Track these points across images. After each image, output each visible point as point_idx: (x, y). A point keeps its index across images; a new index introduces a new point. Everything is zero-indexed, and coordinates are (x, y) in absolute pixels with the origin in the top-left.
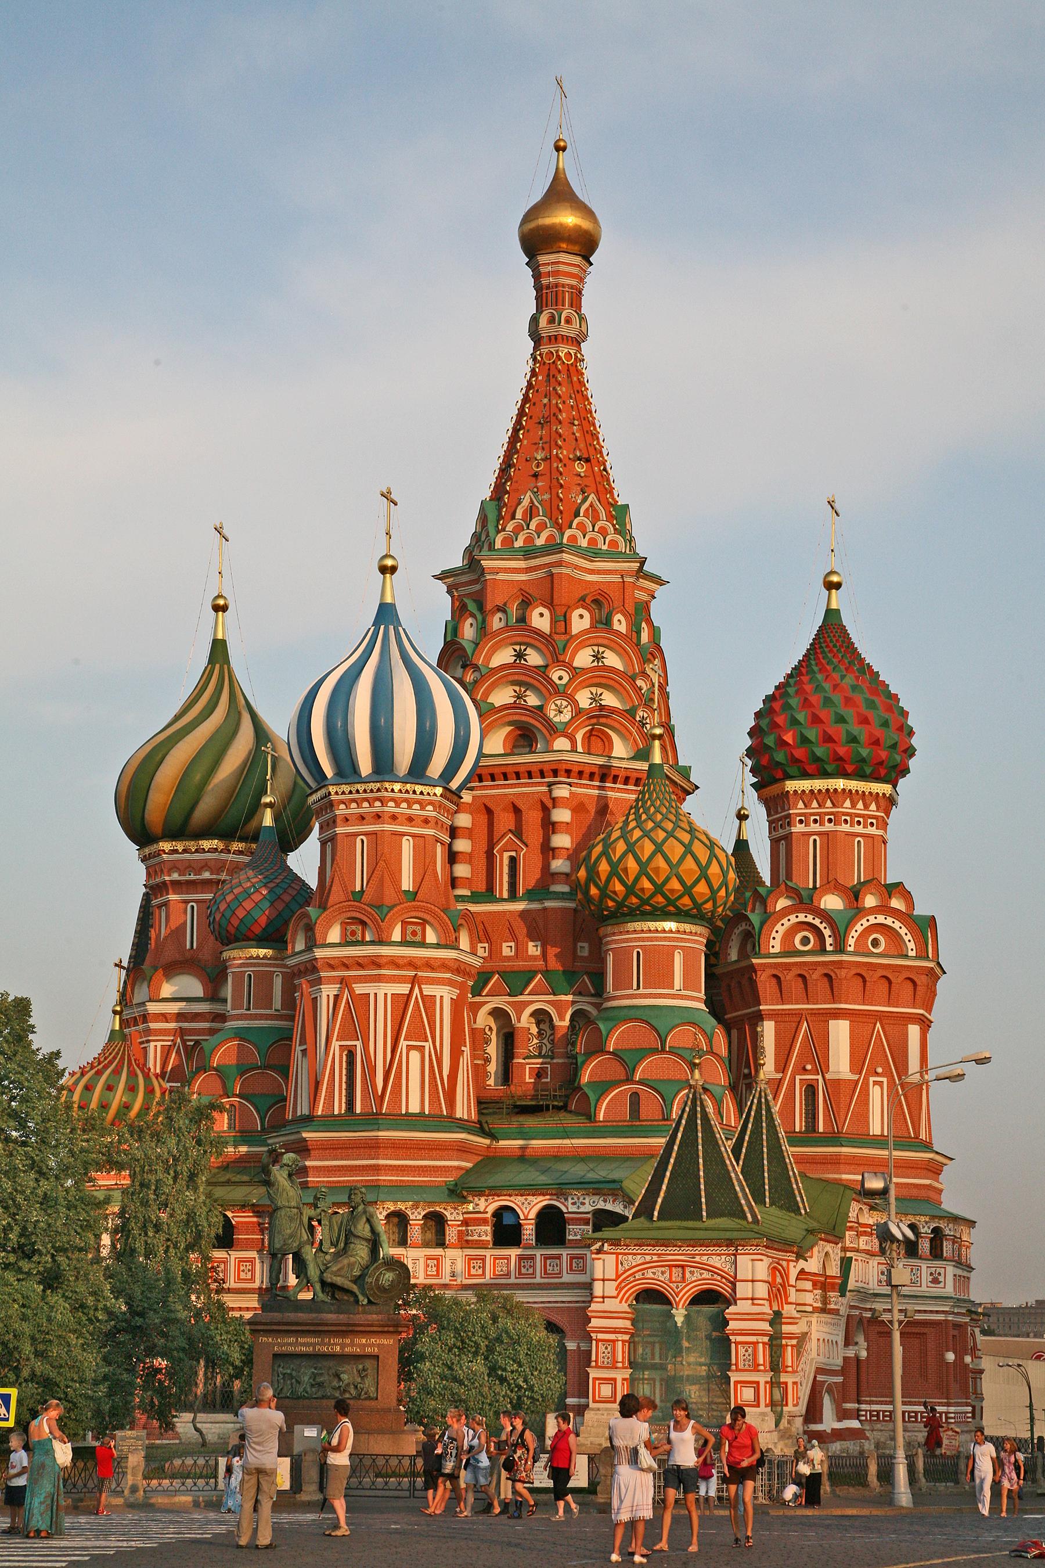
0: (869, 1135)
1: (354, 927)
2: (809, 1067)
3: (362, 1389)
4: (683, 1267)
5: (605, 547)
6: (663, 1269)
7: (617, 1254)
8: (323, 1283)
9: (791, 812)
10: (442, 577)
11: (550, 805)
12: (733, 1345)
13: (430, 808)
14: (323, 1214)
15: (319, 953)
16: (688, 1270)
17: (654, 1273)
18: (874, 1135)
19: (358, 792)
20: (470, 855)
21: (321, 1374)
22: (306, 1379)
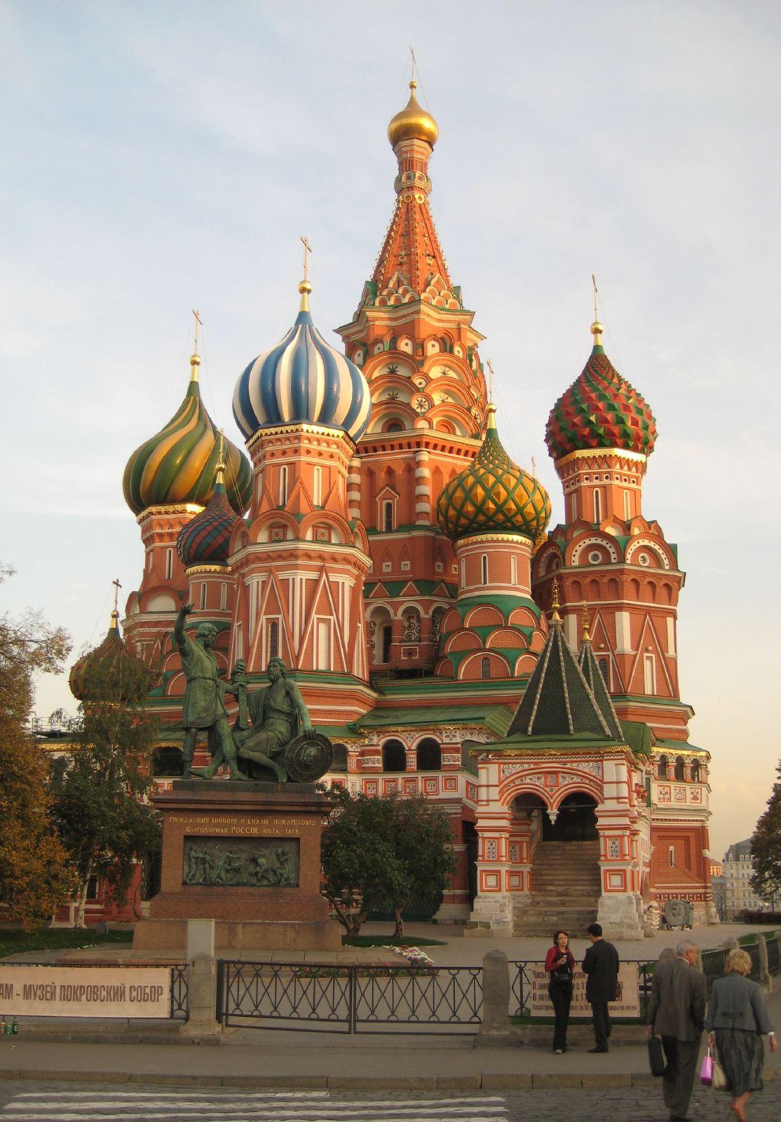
0: (644, 694)
1: (276, 530)
2: (602, 646)
3: (282, 875)
6: (539, 775)
9: (580, 472)
10: (338, 331)
11: (413, 465)
12: (602, 840)
13: (334, 446)
14: (240, 689)
15: (251, 549)
16: (560, 775)
19: (282, 432)
20: (359, 503)
21: (238, 858)
22: (221, 863)
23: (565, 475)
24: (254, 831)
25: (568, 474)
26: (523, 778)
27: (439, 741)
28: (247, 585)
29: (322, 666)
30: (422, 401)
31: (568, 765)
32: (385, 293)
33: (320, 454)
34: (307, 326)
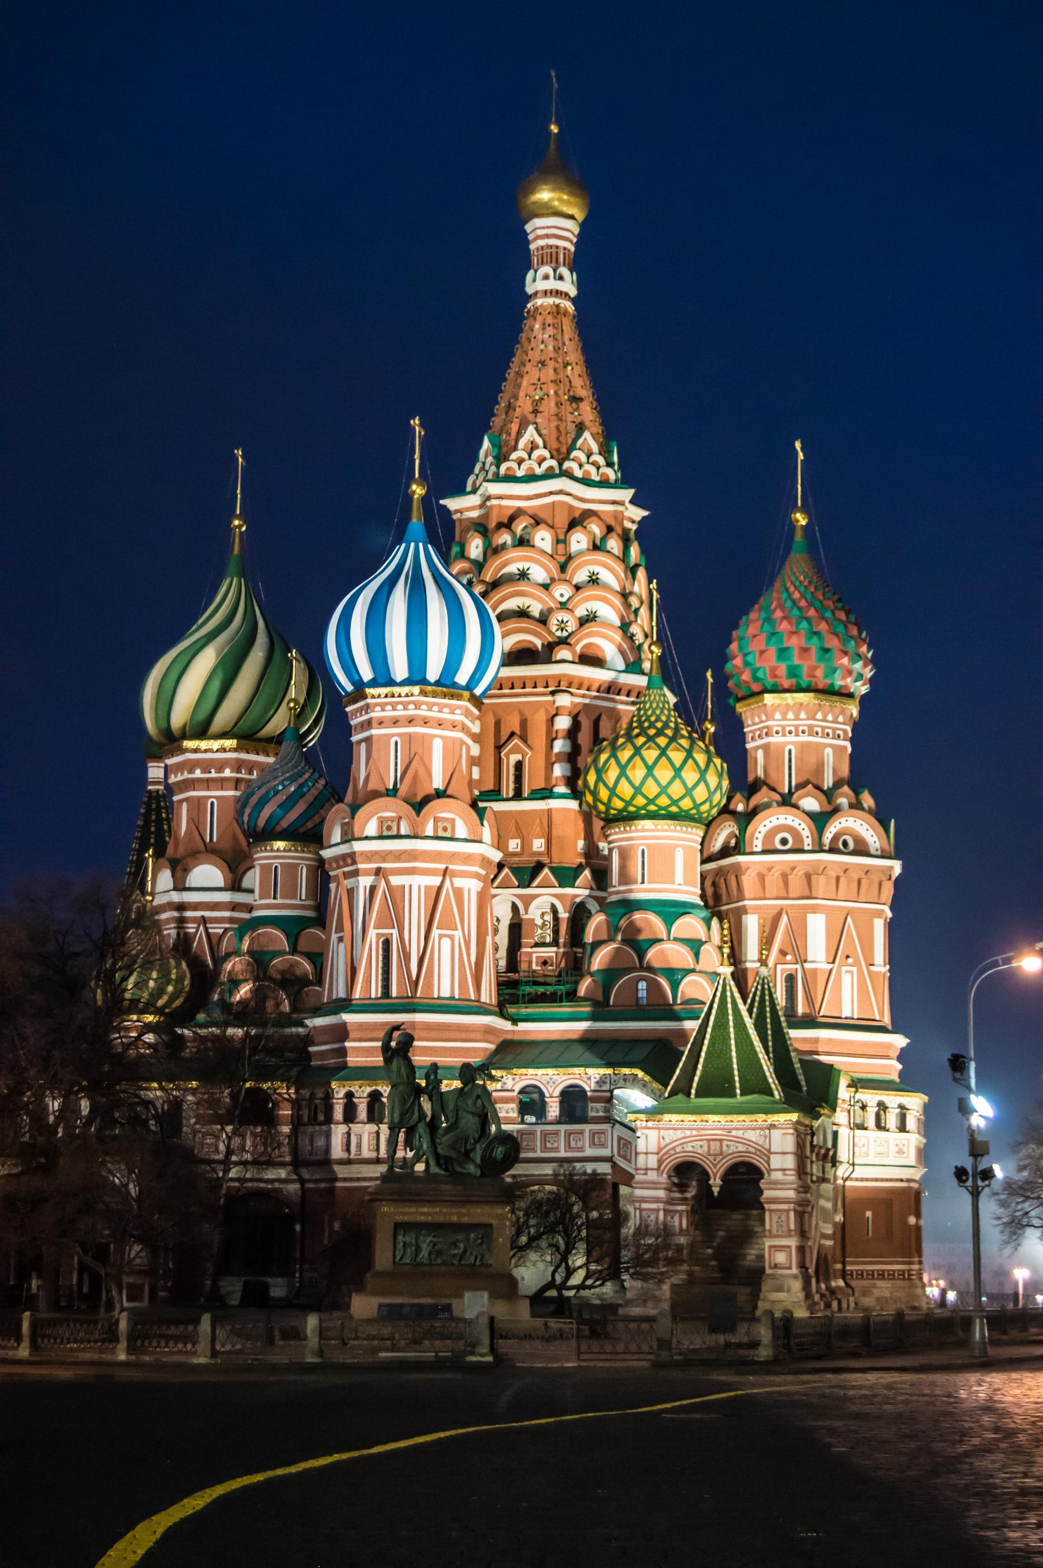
2: (789, 957)
4: (721, 1140)
5: (597, 479)
7: (659, 1129)
8: (437, 1156)
13: (458, 711)
15: (358, 846)
16: (725, 1143)
17: (693, 1147)
18: (846, 1018)
23: (750, 722)
24: (455, 1219)
25: (755, 724)
26: (685, 1145)
27: (587, 1088)
28: (349, 887)
29: (446, 993)
30: (562, 621)
31: (734, 1133)
32: (514, 456)
33: (440, 724)
34: (421, 545)
